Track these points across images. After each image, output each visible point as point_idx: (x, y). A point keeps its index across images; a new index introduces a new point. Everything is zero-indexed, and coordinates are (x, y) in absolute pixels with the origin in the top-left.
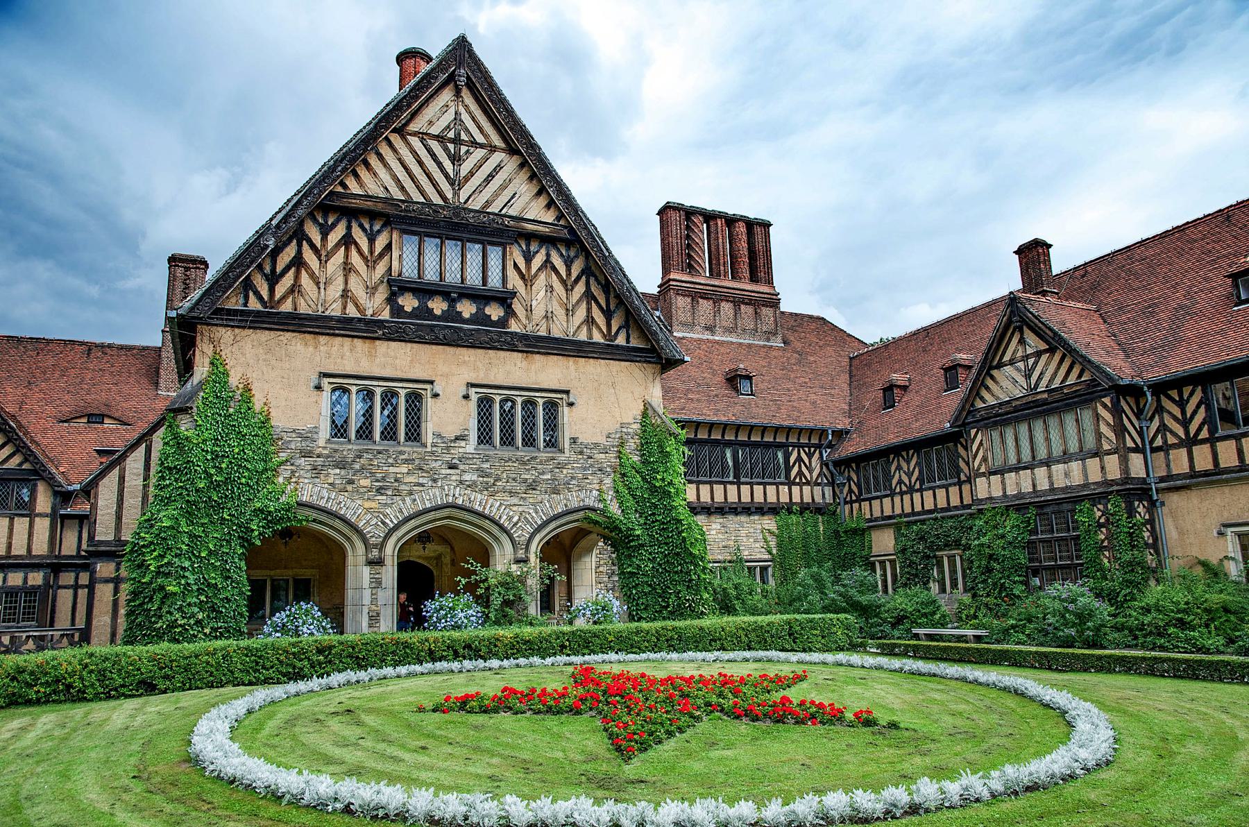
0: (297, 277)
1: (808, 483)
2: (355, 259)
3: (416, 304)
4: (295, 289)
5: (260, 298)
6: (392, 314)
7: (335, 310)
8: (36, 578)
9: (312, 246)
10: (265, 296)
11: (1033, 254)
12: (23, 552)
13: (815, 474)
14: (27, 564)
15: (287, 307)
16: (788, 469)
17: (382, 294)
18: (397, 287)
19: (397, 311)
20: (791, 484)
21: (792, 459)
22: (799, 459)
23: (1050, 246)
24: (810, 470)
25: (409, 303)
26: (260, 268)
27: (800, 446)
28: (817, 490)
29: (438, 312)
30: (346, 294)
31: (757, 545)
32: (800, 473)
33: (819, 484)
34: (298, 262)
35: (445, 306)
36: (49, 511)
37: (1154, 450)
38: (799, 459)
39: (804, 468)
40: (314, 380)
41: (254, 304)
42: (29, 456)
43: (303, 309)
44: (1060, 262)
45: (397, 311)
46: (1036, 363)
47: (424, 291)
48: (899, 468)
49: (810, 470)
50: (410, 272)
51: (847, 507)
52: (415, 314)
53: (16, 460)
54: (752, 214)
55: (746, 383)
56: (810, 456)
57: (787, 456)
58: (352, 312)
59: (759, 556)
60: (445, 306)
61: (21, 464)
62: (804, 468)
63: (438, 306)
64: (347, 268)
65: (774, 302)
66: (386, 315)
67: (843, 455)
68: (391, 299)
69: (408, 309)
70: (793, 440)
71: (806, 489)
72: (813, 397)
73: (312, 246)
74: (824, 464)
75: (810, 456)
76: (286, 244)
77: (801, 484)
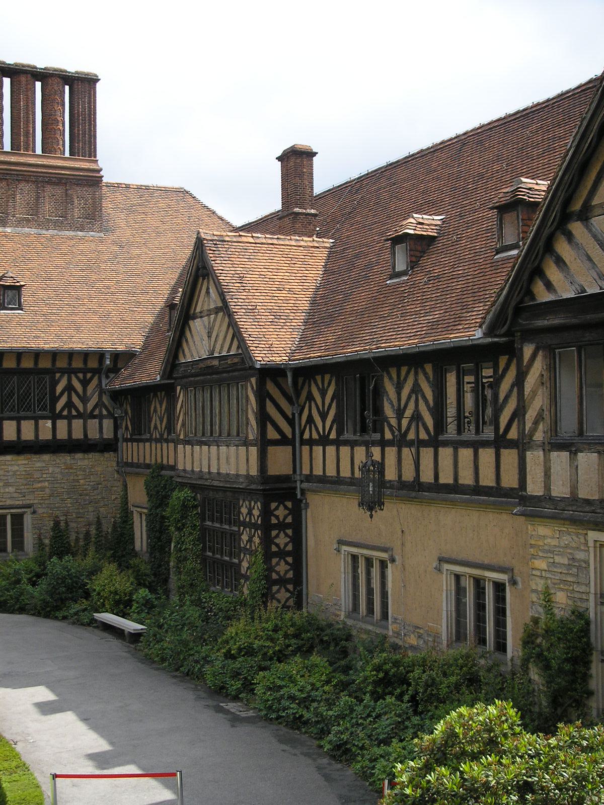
1: (80, 416)
11: (297, 162)
13: (90, 406)
16: (55, 399)
20: (55, 417)
21: (59, 388)
22: (70, 388)
23: (311, 154)
24: (84, 399)
27: (70, 371)
28: (93, 424)
31: (11, 489)
32: (69, 404)
33: (94, 417)
37: (303, 442)
38: (70, 388)
39: (75, 399)
44: (325, 177)
46: (215, 320)
48: (155, 411)
49: (84, 399)
51: (125, 444)
54: (72, 66)
55: (10, 293)
56: (85, 383)
57: (55, 383)
59: (9, 502)
62: (75, 399)
65: (93, 180)
67: (129, 384)
70: (62, 364)
71: (77, 424)
72: (111, 307)
74: (102, 392)
75: (85, 383)
77: (69, 418)
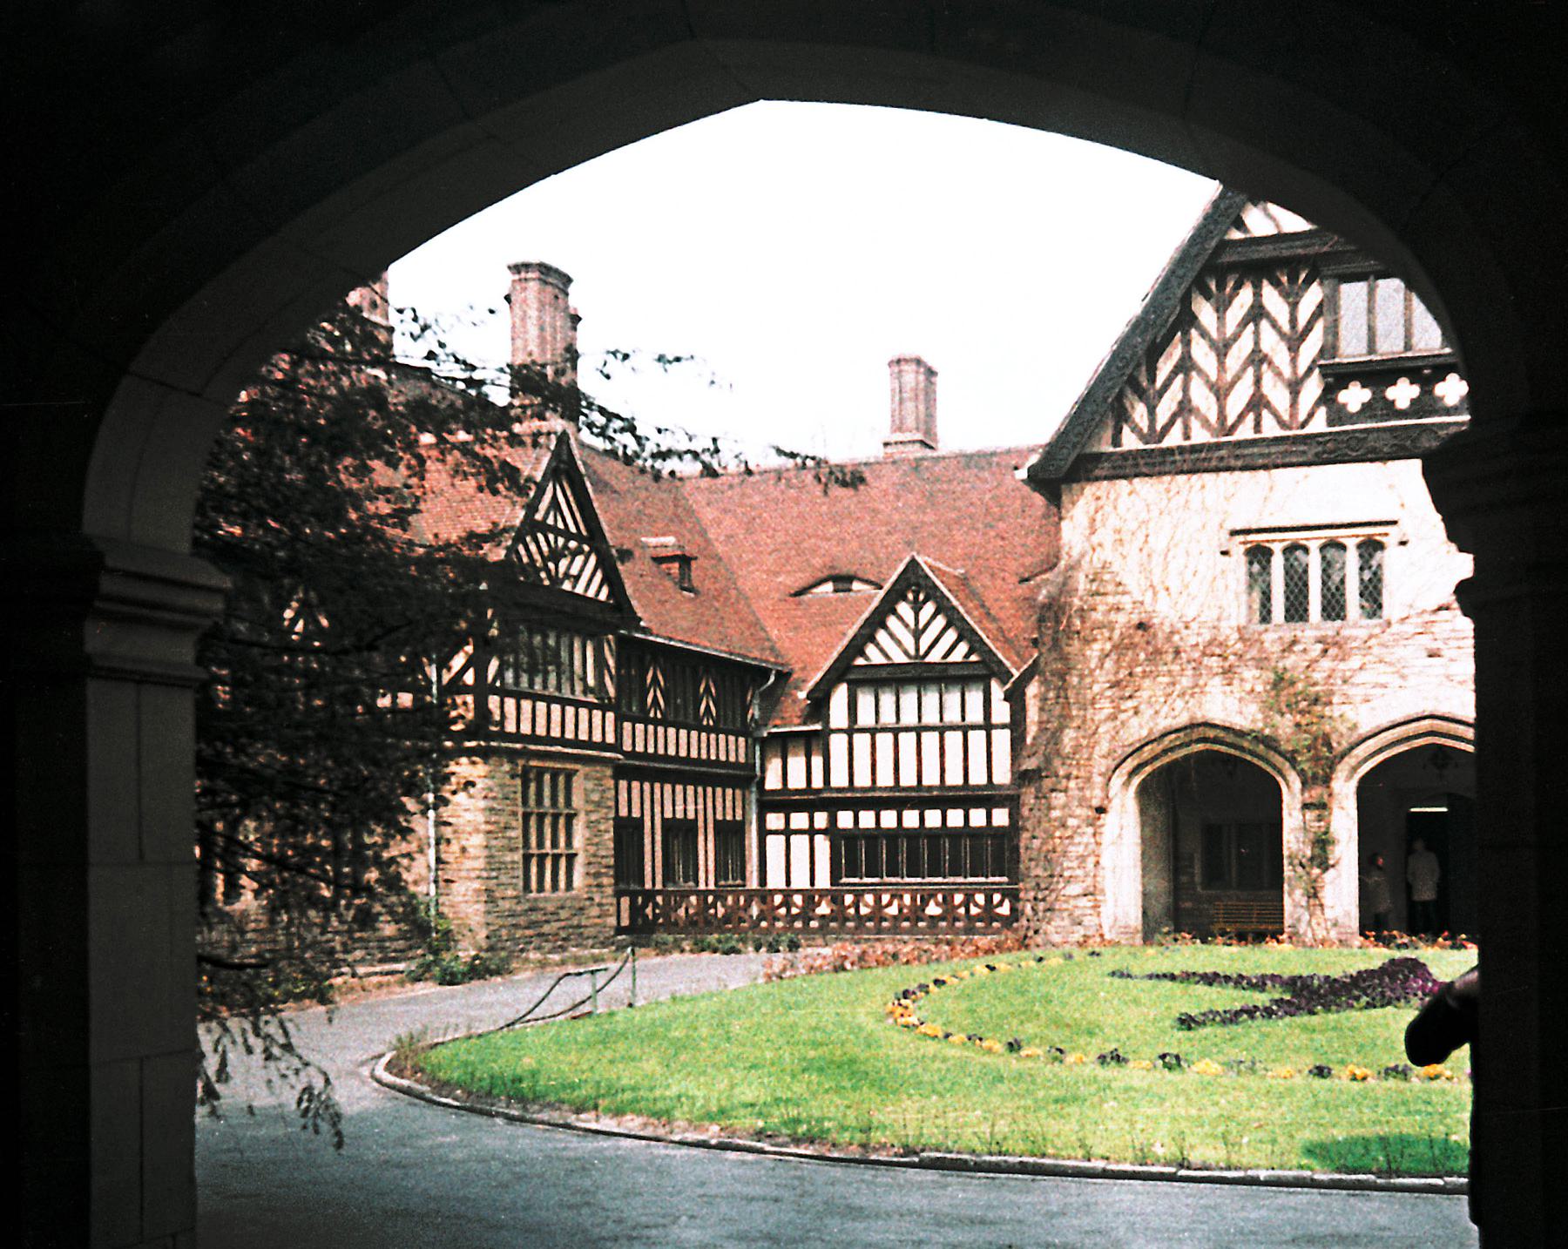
0: (1186, 388)
2: (1271, 343)
3: (1366, 395)
4: (1185, 408)
5: (1136, 429)
6: (1330, 423)
7: (1245, 432)
8: (1001, 817)
9: (1204, 334)
10: (1144, 424)
12: (983, 781)
14: (986, 798)
15: (1174, 439)
17: (1313, 388)
18: (1337, 377)
19: (1338, 415)
25: (1355, 396)
26: (1133, 383)
29: (1403, 403)
30: (1257, 403)
34: (1186, 366)
35: (1415, 391)
36: (1007, 720)
40: (1224, 540)
41: (1130, 442)
42: (976, 645)
43: (1200, 436)
45: (1338, 415)
47: (1378, 374)
50: (1352, 349)
52: (1367, 410)
53: (963, 648)
58: (1271, 429)
60: (1415, 391)
61: (967, 656)
63: (1403, 393)
64: (1258, 359)
66: (1319, 425)
68: (1328, 397)
69: (1354, 407)
73: (1204, 334)
76: (1168, 340)
